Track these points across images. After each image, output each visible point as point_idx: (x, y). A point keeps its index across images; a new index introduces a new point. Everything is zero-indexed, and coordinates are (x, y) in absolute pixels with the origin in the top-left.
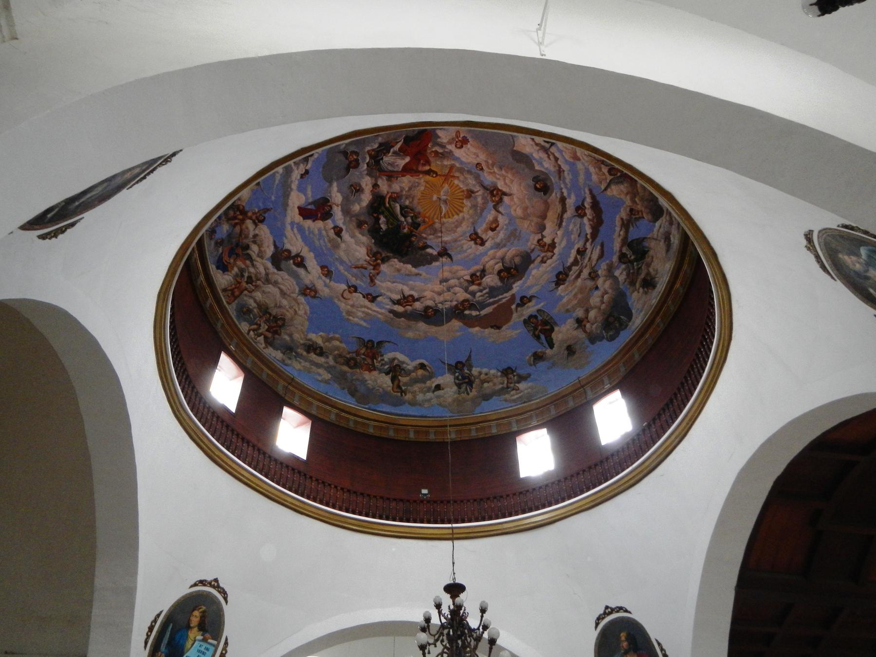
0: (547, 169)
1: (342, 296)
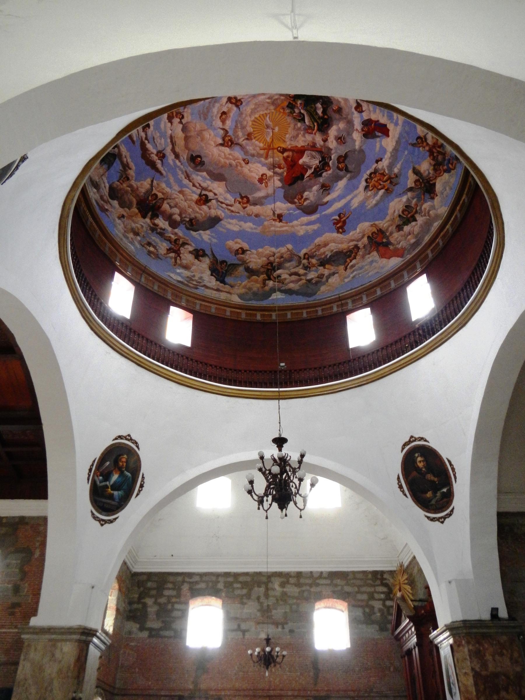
0: (197, 175)
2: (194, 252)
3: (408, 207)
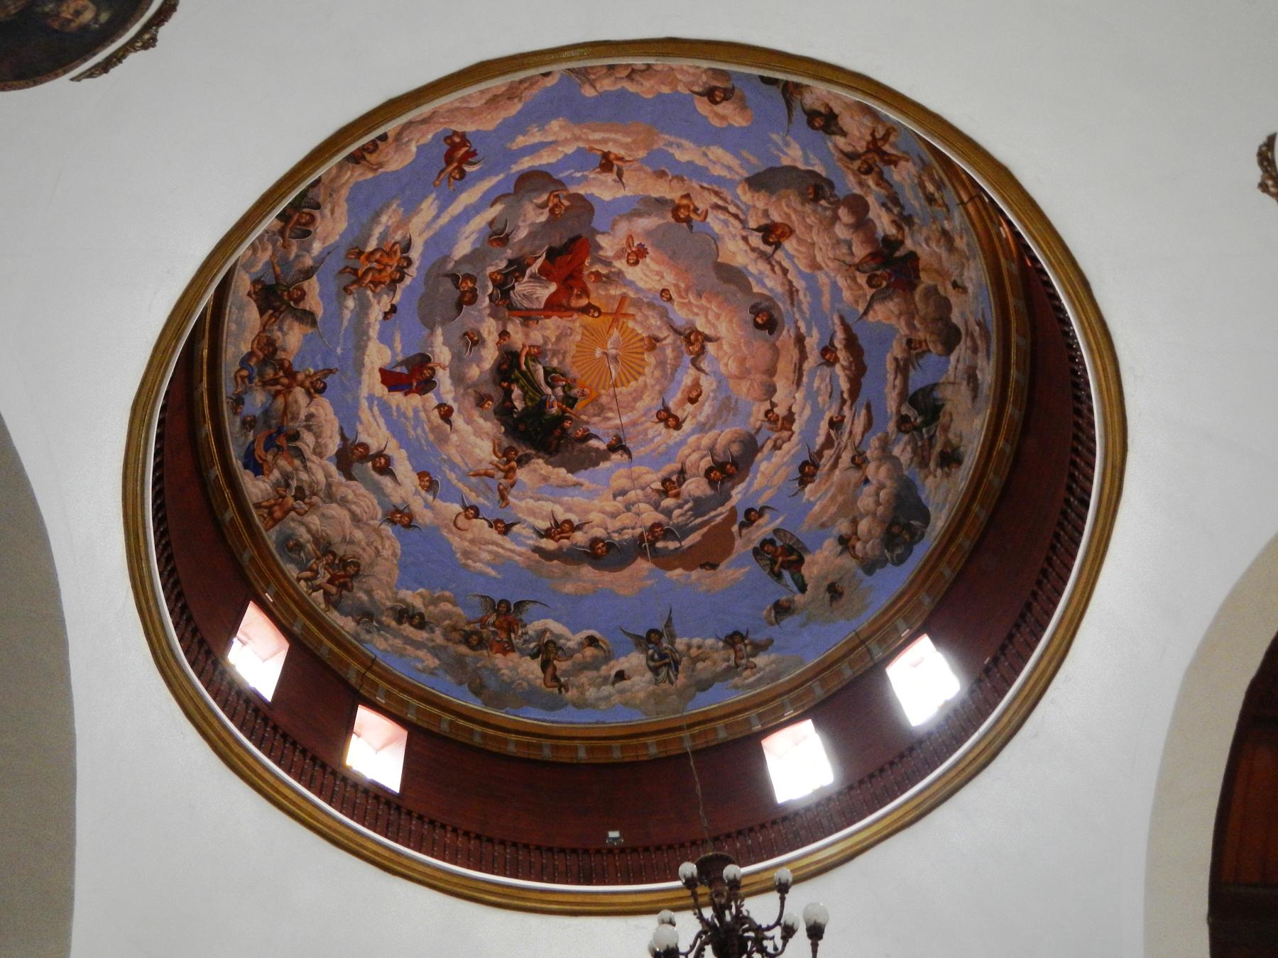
0: (771, 290)
1: (455, 524)
2: (833, 128)
3: (305, 234)
